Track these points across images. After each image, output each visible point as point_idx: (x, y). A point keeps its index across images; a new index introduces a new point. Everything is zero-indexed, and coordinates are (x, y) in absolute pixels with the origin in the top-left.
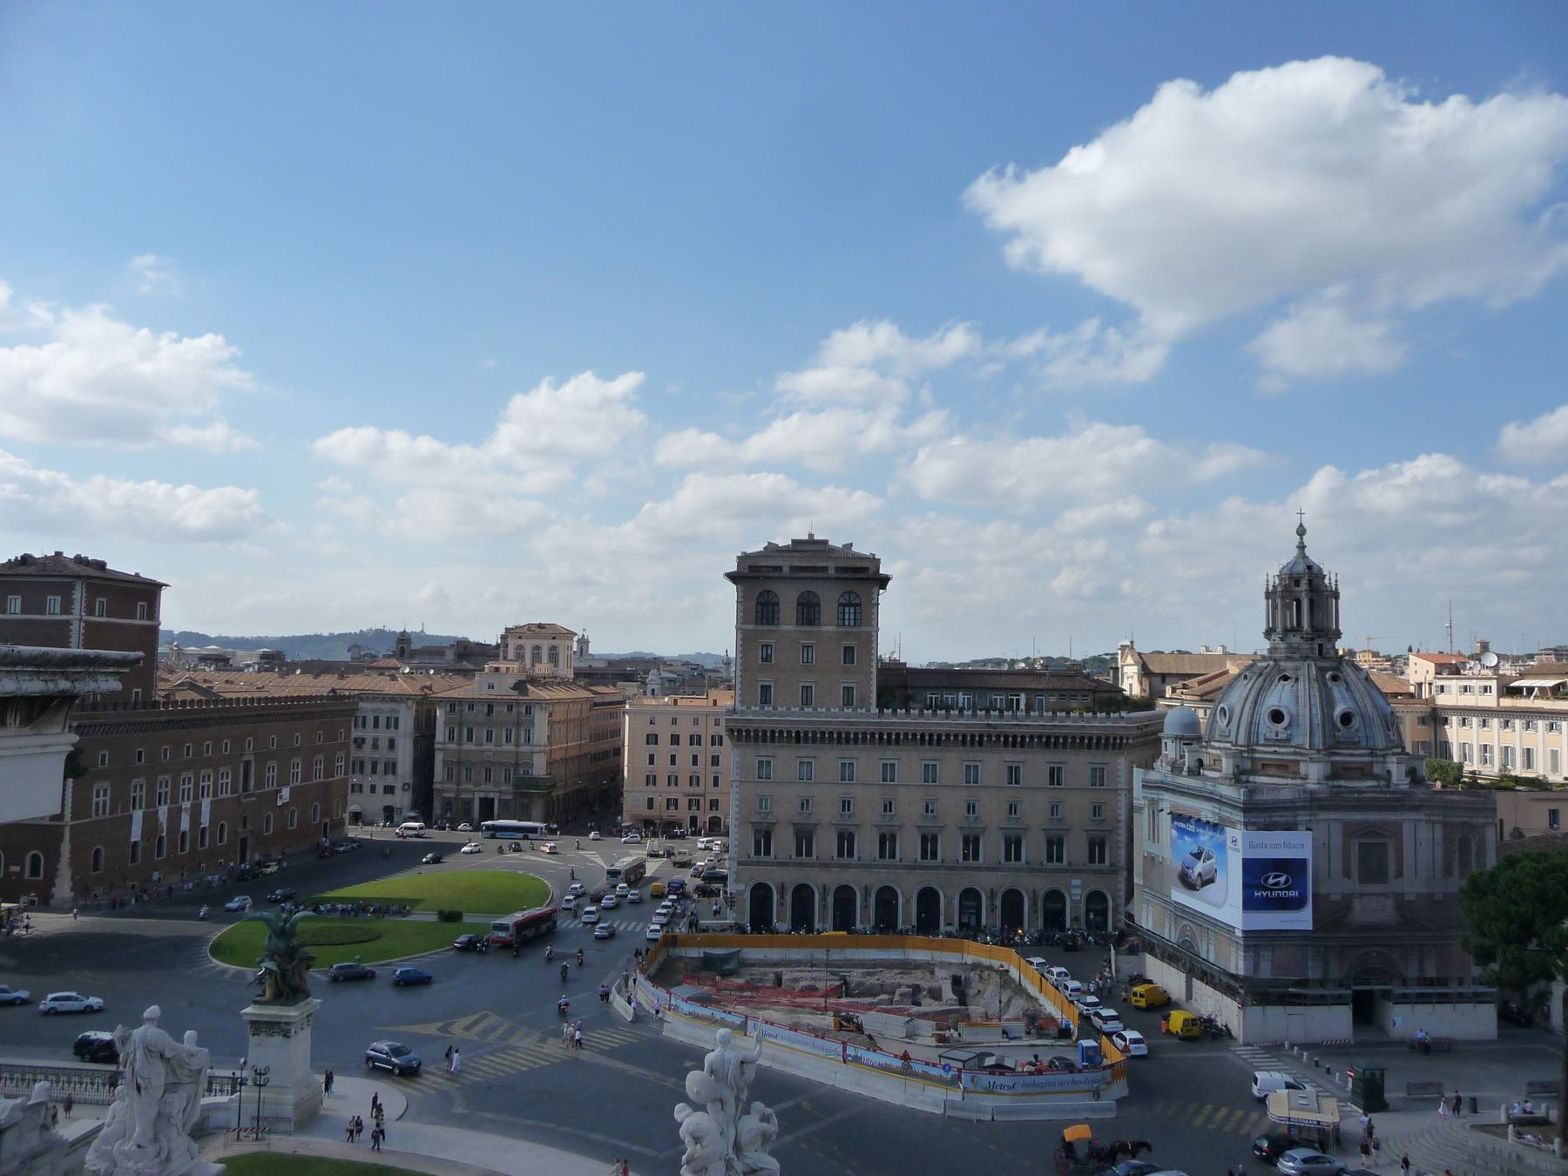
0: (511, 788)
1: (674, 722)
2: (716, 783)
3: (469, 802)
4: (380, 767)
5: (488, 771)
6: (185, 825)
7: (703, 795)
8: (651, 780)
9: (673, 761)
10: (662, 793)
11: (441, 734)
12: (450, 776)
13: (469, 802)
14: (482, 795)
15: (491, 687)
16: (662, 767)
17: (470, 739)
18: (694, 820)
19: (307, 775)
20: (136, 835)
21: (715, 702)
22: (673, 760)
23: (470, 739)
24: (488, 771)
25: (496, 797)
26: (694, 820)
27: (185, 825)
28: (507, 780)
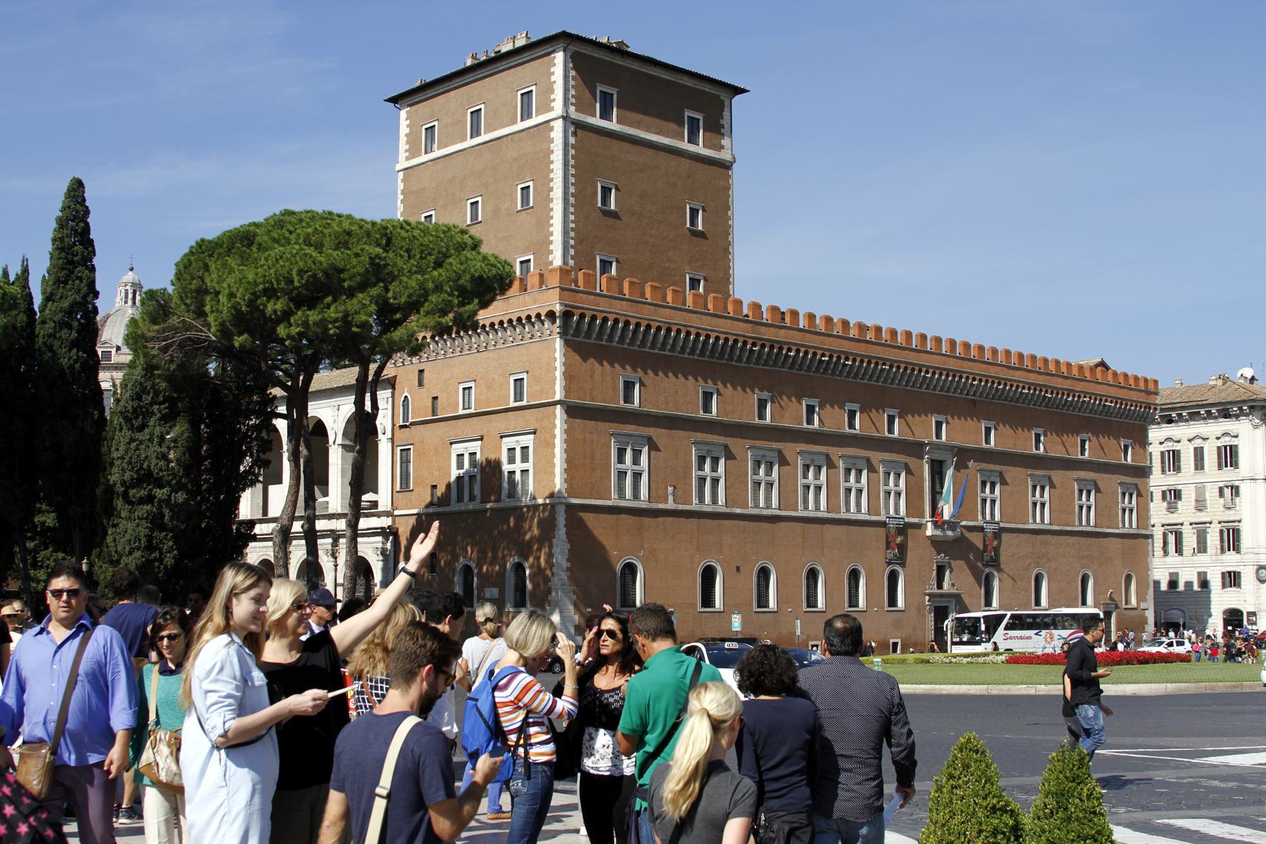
4: (1213, 539)
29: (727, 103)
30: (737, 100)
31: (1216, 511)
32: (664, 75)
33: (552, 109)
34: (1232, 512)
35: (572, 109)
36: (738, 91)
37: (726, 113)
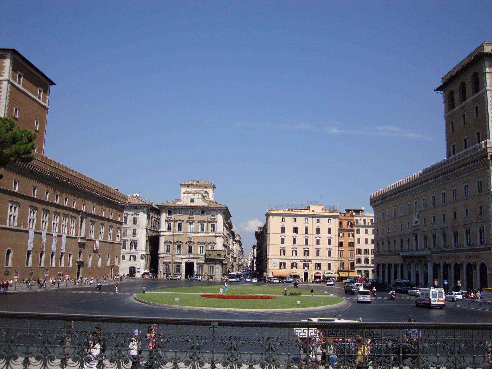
0: (203, 257)
1: (295, 220)
2: (318, 254)
3: (178, 265)
5: (190, 247)
6: (54, 248)
7: (311, 261)
8: (283, 252)
9: (295, 242)
10: (288, 258)
11: (163, 226)
12: (168, 250)
13: (178, 265)
14: (187, 261)
15: (192, 200)
16: (289, 246)
17: (180, 229)
18: (306, 275)
19: (106, 237)
20: (30, 247)
21: (313, 211)
22: (295, 241)
23: (180, 229)
24: (190, 247)
25: (195, 262)
26: (306, 275)
27: (54, 248)
28: (202, 252)
29: (49, 87)
30: (52, 87)
31: (129, 237)
32: (36, 73)
33: (3, 76)
34: (135, 237)
35: (11, 78)
36: (53, 84)
37: (48, 91)
